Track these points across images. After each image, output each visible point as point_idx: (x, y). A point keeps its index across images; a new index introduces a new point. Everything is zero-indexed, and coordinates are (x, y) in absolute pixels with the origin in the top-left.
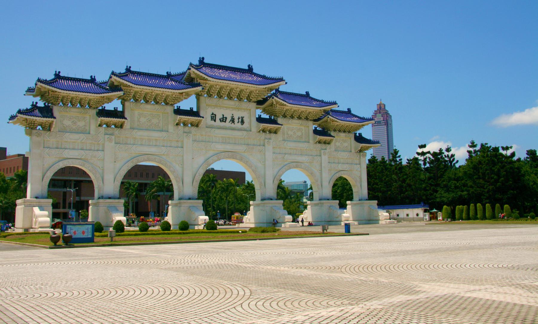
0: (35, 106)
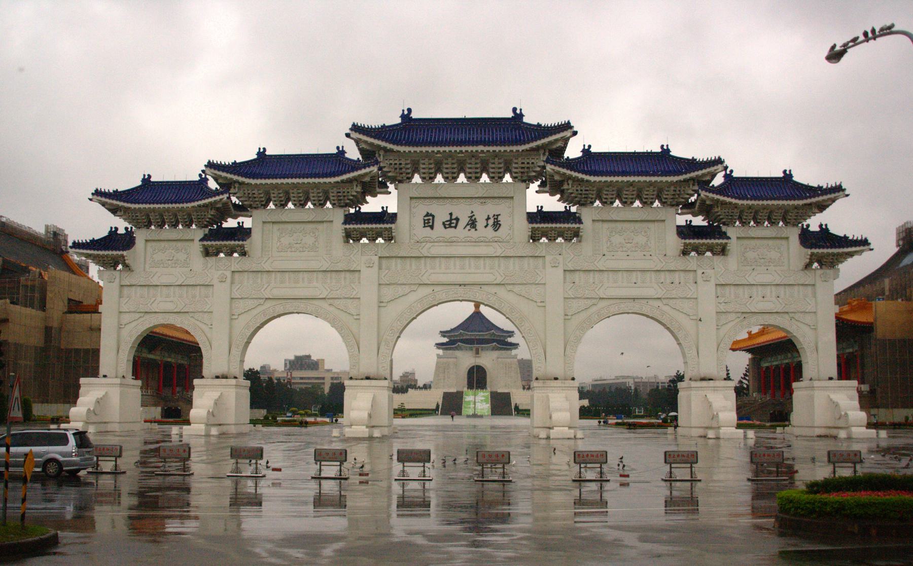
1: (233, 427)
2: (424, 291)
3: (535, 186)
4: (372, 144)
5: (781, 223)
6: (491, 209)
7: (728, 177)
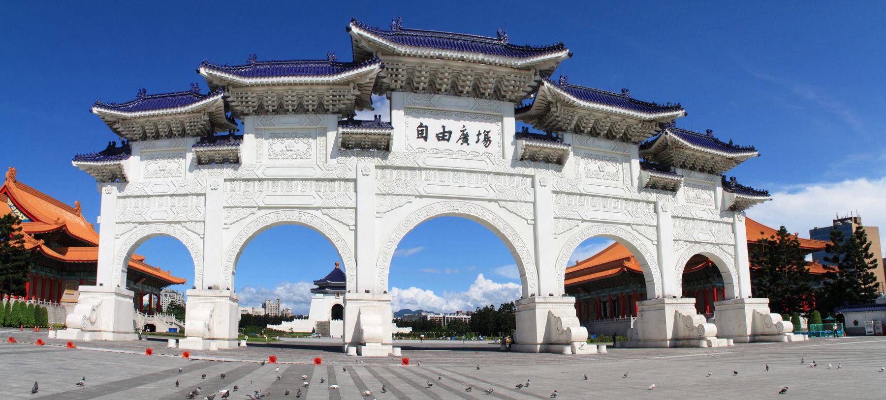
1: (227, 342)
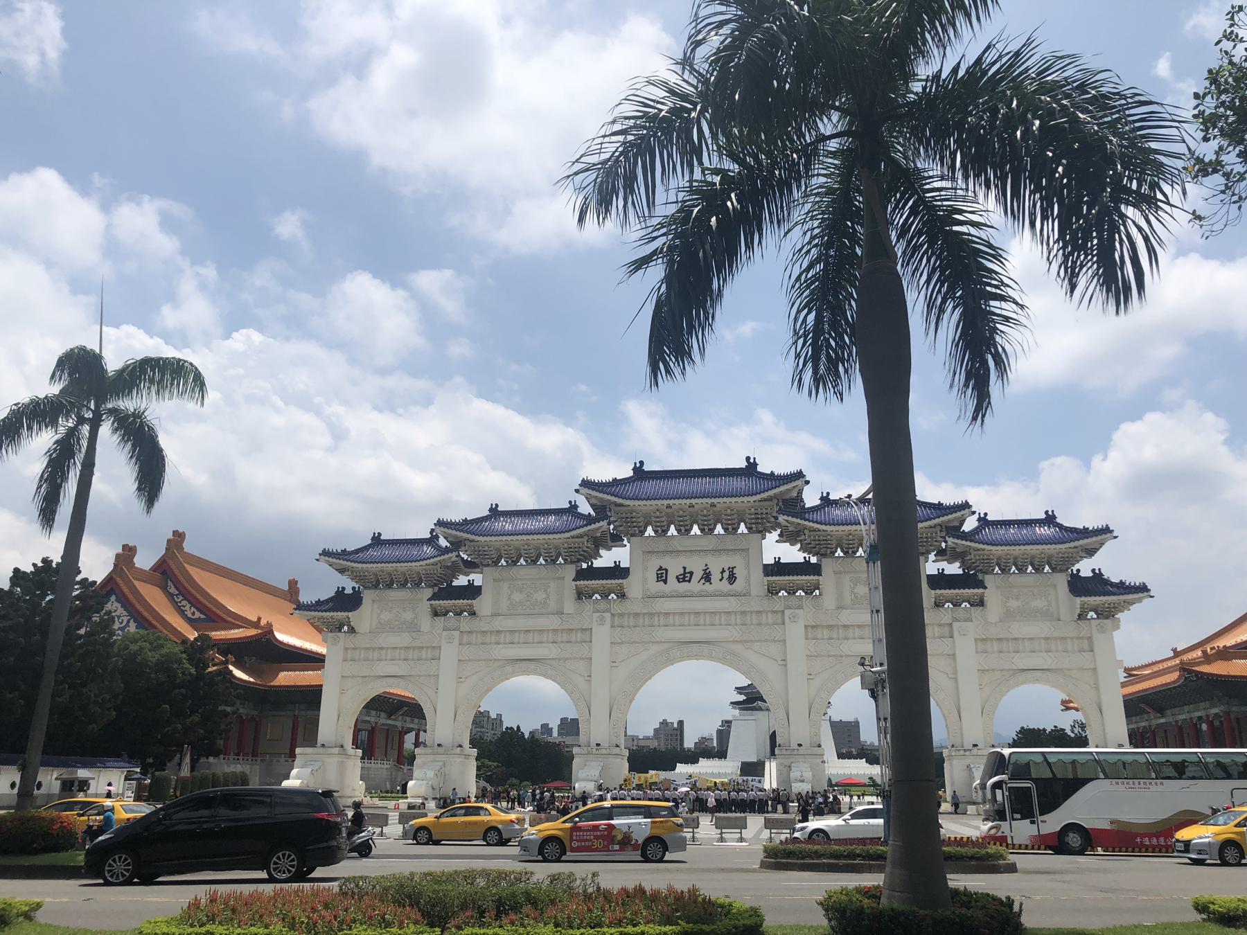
0: (340, 592)
2: (655, 649)
3: (774, 535)
4: (601, 500)
5: (1047, 568)
6: (726, 562)
7: (983, 521)
